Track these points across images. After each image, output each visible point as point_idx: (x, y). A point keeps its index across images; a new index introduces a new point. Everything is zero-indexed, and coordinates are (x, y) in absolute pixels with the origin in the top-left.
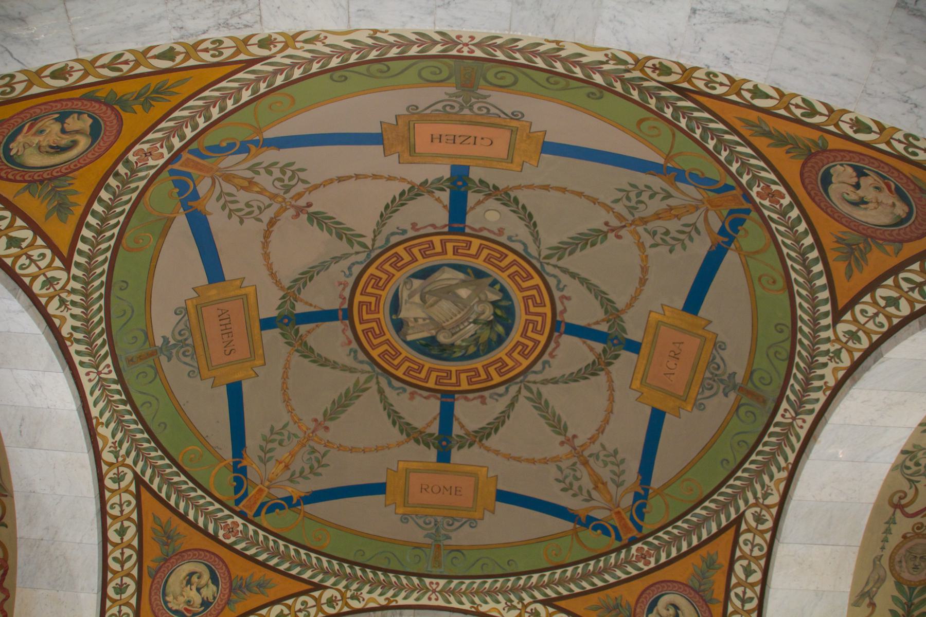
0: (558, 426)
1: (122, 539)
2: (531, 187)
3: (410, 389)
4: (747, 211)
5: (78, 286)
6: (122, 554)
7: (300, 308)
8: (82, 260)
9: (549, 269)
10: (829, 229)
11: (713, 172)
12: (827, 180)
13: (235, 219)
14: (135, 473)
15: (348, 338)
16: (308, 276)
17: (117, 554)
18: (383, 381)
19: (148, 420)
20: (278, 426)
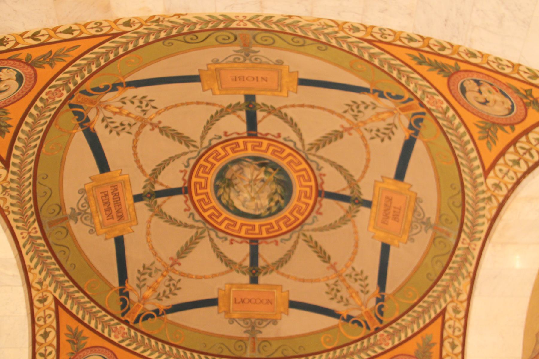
0: (325, 257)
1: (46, 340)
2: (293, 106)
3: (230, 238)
4: (423, 114)
5: (15, 177)
6: (46, 350)
7: (158, 188)
8: (17, 161)
9: (311, 157)
10: (471, 119)
11: (396, 90)
12: (463, 90)
13: (114, 133)
14: (55, 298)
15: (187, 205)
16: (162, 166)
17: (42, 351)
18: (213, 234)
19: (63, 262)
20: (148, 264)
